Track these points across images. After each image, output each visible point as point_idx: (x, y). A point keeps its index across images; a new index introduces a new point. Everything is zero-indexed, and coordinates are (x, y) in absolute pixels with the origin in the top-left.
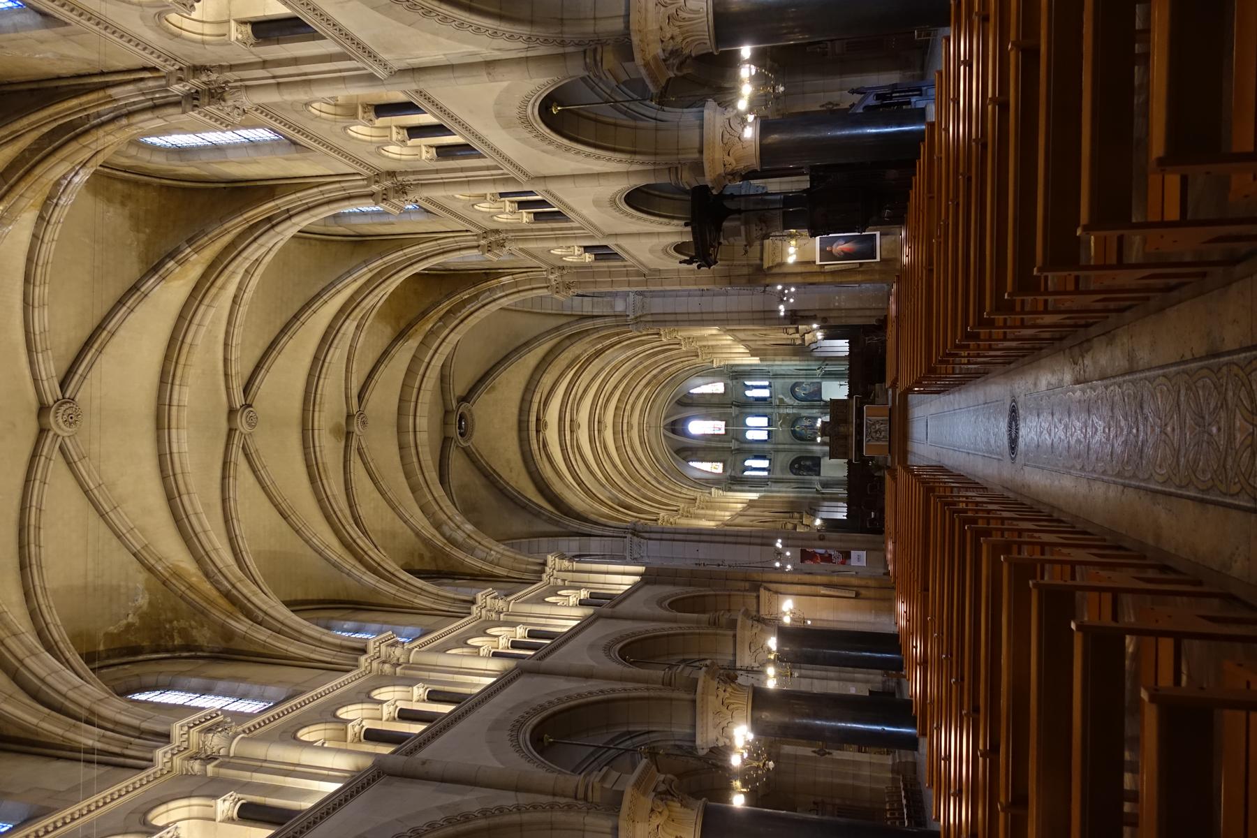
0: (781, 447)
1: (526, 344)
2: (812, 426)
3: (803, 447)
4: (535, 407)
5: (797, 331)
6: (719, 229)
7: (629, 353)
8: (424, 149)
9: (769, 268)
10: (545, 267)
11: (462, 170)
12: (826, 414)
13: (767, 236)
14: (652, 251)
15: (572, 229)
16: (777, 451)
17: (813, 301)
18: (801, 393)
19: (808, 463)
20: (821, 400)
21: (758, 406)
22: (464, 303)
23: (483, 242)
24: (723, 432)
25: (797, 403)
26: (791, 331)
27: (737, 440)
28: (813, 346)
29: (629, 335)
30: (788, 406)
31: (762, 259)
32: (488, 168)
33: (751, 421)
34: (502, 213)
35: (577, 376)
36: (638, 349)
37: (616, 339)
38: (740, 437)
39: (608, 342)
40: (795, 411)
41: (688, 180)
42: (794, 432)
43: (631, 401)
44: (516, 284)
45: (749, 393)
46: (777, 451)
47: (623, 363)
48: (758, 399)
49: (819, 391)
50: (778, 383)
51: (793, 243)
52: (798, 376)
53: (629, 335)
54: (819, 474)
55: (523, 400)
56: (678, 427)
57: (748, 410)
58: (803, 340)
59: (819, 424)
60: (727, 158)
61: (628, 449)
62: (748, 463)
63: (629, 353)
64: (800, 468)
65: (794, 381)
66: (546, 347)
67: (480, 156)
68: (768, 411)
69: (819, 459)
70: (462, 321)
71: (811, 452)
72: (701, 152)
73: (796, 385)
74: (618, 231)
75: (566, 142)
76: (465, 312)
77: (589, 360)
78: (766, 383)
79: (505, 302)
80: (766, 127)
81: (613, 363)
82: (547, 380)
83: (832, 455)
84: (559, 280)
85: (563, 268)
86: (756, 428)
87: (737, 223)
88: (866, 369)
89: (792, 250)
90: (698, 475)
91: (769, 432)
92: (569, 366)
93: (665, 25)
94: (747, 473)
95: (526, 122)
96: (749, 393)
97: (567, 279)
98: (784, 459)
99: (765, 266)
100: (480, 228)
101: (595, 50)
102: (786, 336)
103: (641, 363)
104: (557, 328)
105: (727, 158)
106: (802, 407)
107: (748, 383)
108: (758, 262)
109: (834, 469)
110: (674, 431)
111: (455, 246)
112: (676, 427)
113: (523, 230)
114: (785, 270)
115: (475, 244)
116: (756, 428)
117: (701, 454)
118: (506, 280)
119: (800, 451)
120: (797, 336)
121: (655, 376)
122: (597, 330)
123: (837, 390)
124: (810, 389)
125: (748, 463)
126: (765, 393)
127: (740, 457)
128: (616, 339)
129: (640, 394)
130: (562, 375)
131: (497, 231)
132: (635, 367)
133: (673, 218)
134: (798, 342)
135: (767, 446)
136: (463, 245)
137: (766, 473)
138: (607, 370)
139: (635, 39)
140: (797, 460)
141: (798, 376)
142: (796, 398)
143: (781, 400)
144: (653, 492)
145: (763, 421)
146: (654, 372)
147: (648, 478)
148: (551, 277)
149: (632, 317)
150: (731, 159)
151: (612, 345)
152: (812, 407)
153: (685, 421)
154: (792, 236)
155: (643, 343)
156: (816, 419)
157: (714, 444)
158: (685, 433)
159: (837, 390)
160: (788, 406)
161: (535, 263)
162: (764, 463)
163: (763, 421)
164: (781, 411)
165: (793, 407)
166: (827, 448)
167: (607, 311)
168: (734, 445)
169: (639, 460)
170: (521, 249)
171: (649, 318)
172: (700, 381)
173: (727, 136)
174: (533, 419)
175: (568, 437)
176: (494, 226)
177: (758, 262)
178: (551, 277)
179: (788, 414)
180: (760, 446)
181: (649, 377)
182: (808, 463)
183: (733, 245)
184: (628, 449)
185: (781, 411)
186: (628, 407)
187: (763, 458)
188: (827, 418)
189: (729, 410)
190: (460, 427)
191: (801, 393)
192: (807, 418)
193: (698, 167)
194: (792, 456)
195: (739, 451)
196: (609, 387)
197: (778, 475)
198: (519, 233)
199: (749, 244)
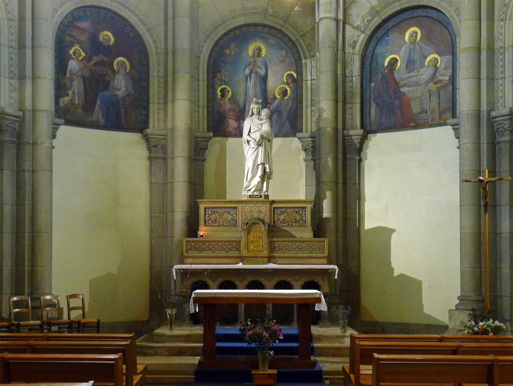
3: (183, 62)
18: (394, 54)
19: (121, 85)
20: (368, 131)
40: (325, 28)
49: (401, 117)
64: (95, 47)
69: (140, 126)
106: (339, 60)
119: (170, 53)
140: (131, 43)
142: (385, 28)
152: (341, 97)
165: (342, 23)
182: (121, 85)
191: (394, 54)
192: (297, 83)
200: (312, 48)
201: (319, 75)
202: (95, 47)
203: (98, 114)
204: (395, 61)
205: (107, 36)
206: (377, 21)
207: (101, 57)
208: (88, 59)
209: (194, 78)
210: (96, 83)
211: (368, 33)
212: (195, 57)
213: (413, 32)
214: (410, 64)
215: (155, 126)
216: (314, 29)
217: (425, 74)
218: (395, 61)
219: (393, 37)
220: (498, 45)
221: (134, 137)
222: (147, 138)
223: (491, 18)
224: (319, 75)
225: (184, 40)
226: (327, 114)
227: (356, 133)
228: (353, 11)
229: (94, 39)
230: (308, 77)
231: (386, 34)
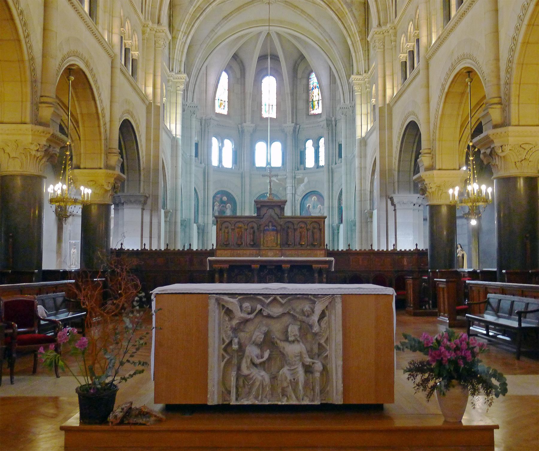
24: (265, 115)
25: (299, 198)
27: (255, 130)
30: (295, 188)
33: (277, 147)
45: (309, 144)
46: (242, 177)
50: (324, 177)
57: (289, 142)
64: (222, 202)
65: (325, 195)
73: (320, 196)
78: (322, 163)
96: (309, 144)
106: (293, 205)
107: (322, 142)
110: (262, 58)
116: (269, 154)
119: (243, 203)
126: (310, 163)
140: (232, 200)
142: (306, 196)
143: (301, 181)
145: (277, 162)
153: (277, 73)
157: (249, 102)
162: (228, 163)
163: (277, 162)
164: (289, 181)
168: (248, 125)
179: (285, 189)
185: (289, 181)
194: (236, 194)
195: (242, 132)
197: (212, 178)
202: (222, 202)
204: (309, 206)
205: (225, 198)
206: (304, 194)
207: (223, 204)
208: (219, 206)
211: (302, 197)
213: (314, 198)
218: (309, 206)
219: (309, 198)
220: (334, 206)
223: (332, 199)
228: (297, 191)
229: (221, 199)
231: (307, 197)
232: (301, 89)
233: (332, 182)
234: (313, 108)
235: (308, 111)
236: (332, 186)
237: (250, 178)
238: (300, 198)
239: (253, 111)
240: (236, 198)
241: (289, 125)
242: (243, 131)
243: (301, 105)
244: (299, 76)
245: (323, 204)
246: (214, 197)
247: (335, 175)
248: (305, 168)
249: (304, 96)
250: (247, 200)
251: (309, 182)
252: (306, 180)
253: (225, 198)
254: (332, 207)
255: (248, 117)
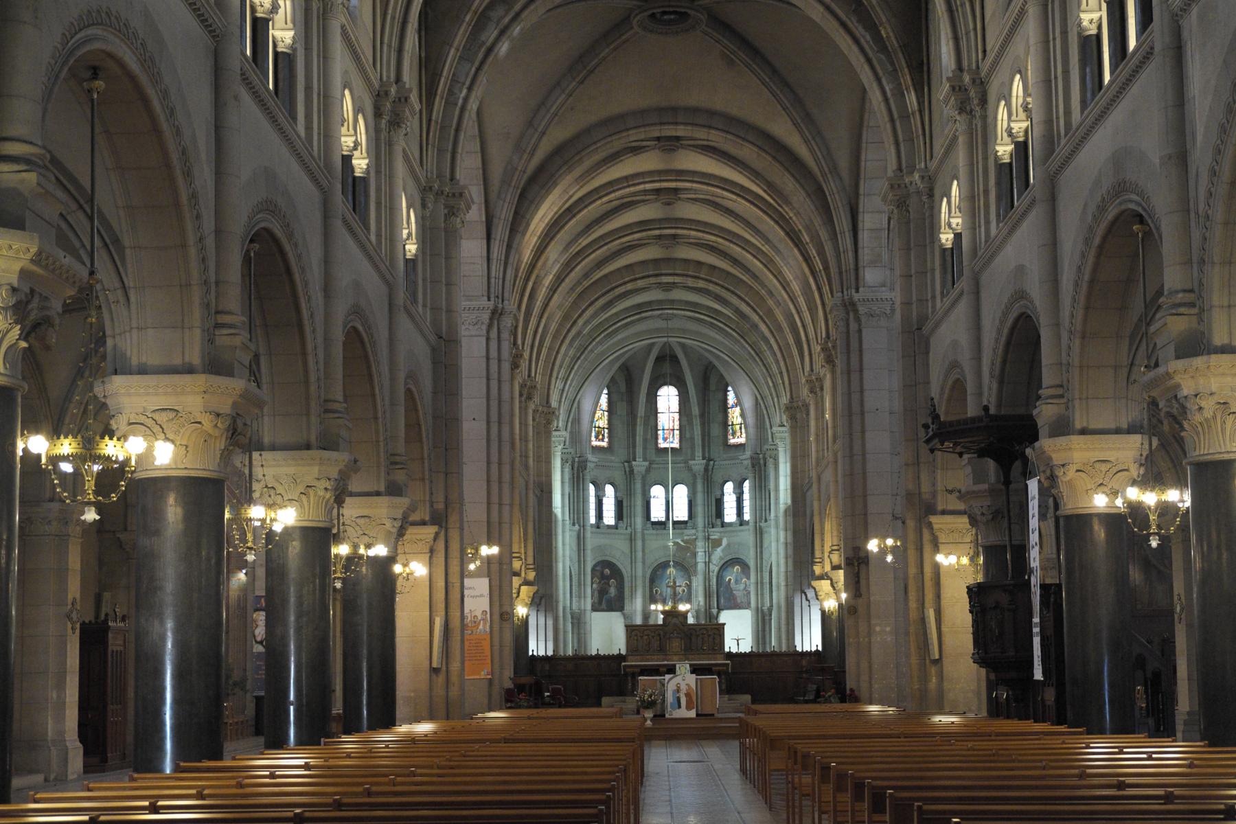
0: (639, 543)
1: (808, 118)
2: (676, 599)
3: (639, 583)
4: (701, 134)
5: (835, 568)
6: (982, 453)
7: (796, 287)
8: (1095, 16)
9: (930, 525)
10: (933, 165)
11: (1066, 72)
12: (697, 617)
13: (973, 522)
14: (955, 344)
15: (988, 222)
16: (632, 539)
17: (881, 591)
18: (731, 575)
19: (613, 591)
20: (720, 609)
21: (707, 504)
22: (872, 28)
23: (967, 79)
24: (662, 444)
25: (715, 569)
26: (836, 558)
27: (648, 470)
28: (810, 594)
29: (826, 289)
30: (709, 554)
31: (943, 513)
32: (1068, 113)
33: (681, 493)
34: (1010, 115)
35: (754, 199)
36: (801, 300)
37: (819, 265)
38: (653, 475)
39: (813, 252)
40: (701, 567)
41: (1045, 413)
42: (665, 565)
43: (711, 287)
44: (905, 117)
45: (729, 487)
46: (632, 539)
47: (778, 275)
48: (719, 503)
49: (735, 606)
50: (748, 536)
51: (965, 560)
52: (759, 569)
53: (826, 289)
54: (594, 609)
55: (712, 113)
56: (667, 368)
57: (700, 487)
58: (821, 578)
59: (683, 607)
60: (1075, 467)
61: (629, 287)
62: (609, 490)
63: (796, 287)
64: (603, 577)
65: (752, 564)
66: (803, 151)
67: (1084, 104)
68: (700, 521)
69: (621, 608)
70: (843, 25)
71: (632, 596)
72: (1084, 432)
73: (745, 567)
74: (983, 295)
75: (1097, 241)
76: (859, 31)
77: (782, 221)
78: (747, 517)
79: (875, 96)
80: (1113, 520)
81: (777, 259)
82: (747, 152)
83: (631, 629)
84: (912, 189)
85: (931, 195)
86: (670, 502)
87: (993, 479)
88: (771, 677)
89: (952, 559)
90: (587, 405)
91: (661, 525)
92: (770, 186)
93: (1216, 398)
94: (592, 488)
95: (1121, 188)
96: (729, 487)
97: (913, 201)
98: (618, 550)
99: (934, 519)
100: (989, 74)
101: (1192, 305)
102: (827, 549)
103: (778, 304)
104: (834, 169)
105: (1073, 468)
106: (707, 579)
107: (747, 484)
108: (940, 508)
109: (607, 635)
110: (660, 359)
111: (962, 31)
112: (667, 368)
113: (985, 143)
114: (927, 548)
115: (965, 64)
117: (622, 409)
118: (912, 99)
119: (633, 578)
120: (828, 568)
121: (755, 326)
122: (834, 236)
123: (738, 633)
124: (738, 590)
125: (609, 490)
126: (730, 515)
127: (618, 476)
128: (819, 265)
129: (725, 302)
130: (755, 174)
131: (984, 101)
132: (771, 293)
133: (1001, 382)
134: (817, 570)
135: (639, 521)
136: (963, 44)
137: (593, 520)
138: (766, 248)
139: (1199, 361)
140: (616, 573)
141: (759, 569)
142: (725, 566)
143: (717, 543)
144: (558, 331)
146: (763, 327)
147: (581, 322)
148: (917, 176)
149: (856, 297)
150: (1071, 473)
151: (807, 259)
152: (708, 595)
154: (972, 559)
155: (812, 310)
156: (689, 600)
158: (657, 383)
159: (738, 633)
160: (709, 554)
161: (939, 151)
162: (609, 518)
165: (707, 564)
166: (638, 621)
167: (865, 255)
168: (640, 465)
169: (610, 304)
170: (955, 138)
171: (853, 326)
172: (748, 403)
173: (1104, 467)
174: (681, 131)
175: (648, 186)
176: (992, 98)
177: (940, 508)
178: (917, 176)
179: (695, 555)
180: (639, 509)
181: (756, 318)
182: (613, 591)
183: (956, 474)
184: (629, 287)
186: (701, 284)
187: (619, 515)
188: (691, 620)
189: (699, 453)
190: (664, 13)
191: (731, 575)
192: (689, 586)
193: (1062, 428)
195: (631, 473)
196: (736, 250)
198: (983, 134)
199: (962, 496)
200: (695, 572)
201: (698, 584)
203: (604, 606)
205: (607, 571)
209: (644, 587)
210: (602, 592)
212: (644, 577)
214: (737, 582)
215: (627, 608)
216: (696, 564)
217: (742, 586)
219: (729, 569)
221: (618, 614)
222: (624, 615)
224: (698, 584)
225: (640, 572)
226: (702, 603)
227: (715, 611)
228: (713, 557)
229: (602, 573)
230: (694, 585)
232: (714, 407)
233: (761, 547)
234: (734, 433)
235: (726, 439)
236: (761, 552)
237: (643, 541)
238: (716, 569)
239: (645, 440)
240: (623, 570)
241: (698, 464)
242: (632, 471)
243: (716, 430)
244: (713, 387)
245: (749, 578)
246: (593, 570)
247: (765, 536)
248: (723, 524)
249: (720, 417)
250: (640, 572)
251: (728, 545)
252: (725, 542)
253: (607, 571)
254: (762, 583)
255: (639, 450)
